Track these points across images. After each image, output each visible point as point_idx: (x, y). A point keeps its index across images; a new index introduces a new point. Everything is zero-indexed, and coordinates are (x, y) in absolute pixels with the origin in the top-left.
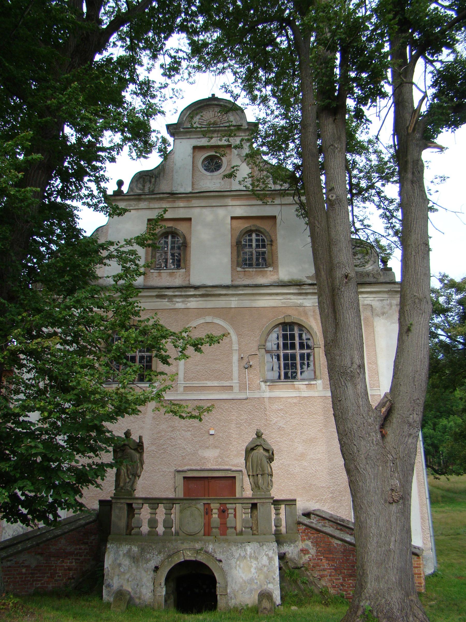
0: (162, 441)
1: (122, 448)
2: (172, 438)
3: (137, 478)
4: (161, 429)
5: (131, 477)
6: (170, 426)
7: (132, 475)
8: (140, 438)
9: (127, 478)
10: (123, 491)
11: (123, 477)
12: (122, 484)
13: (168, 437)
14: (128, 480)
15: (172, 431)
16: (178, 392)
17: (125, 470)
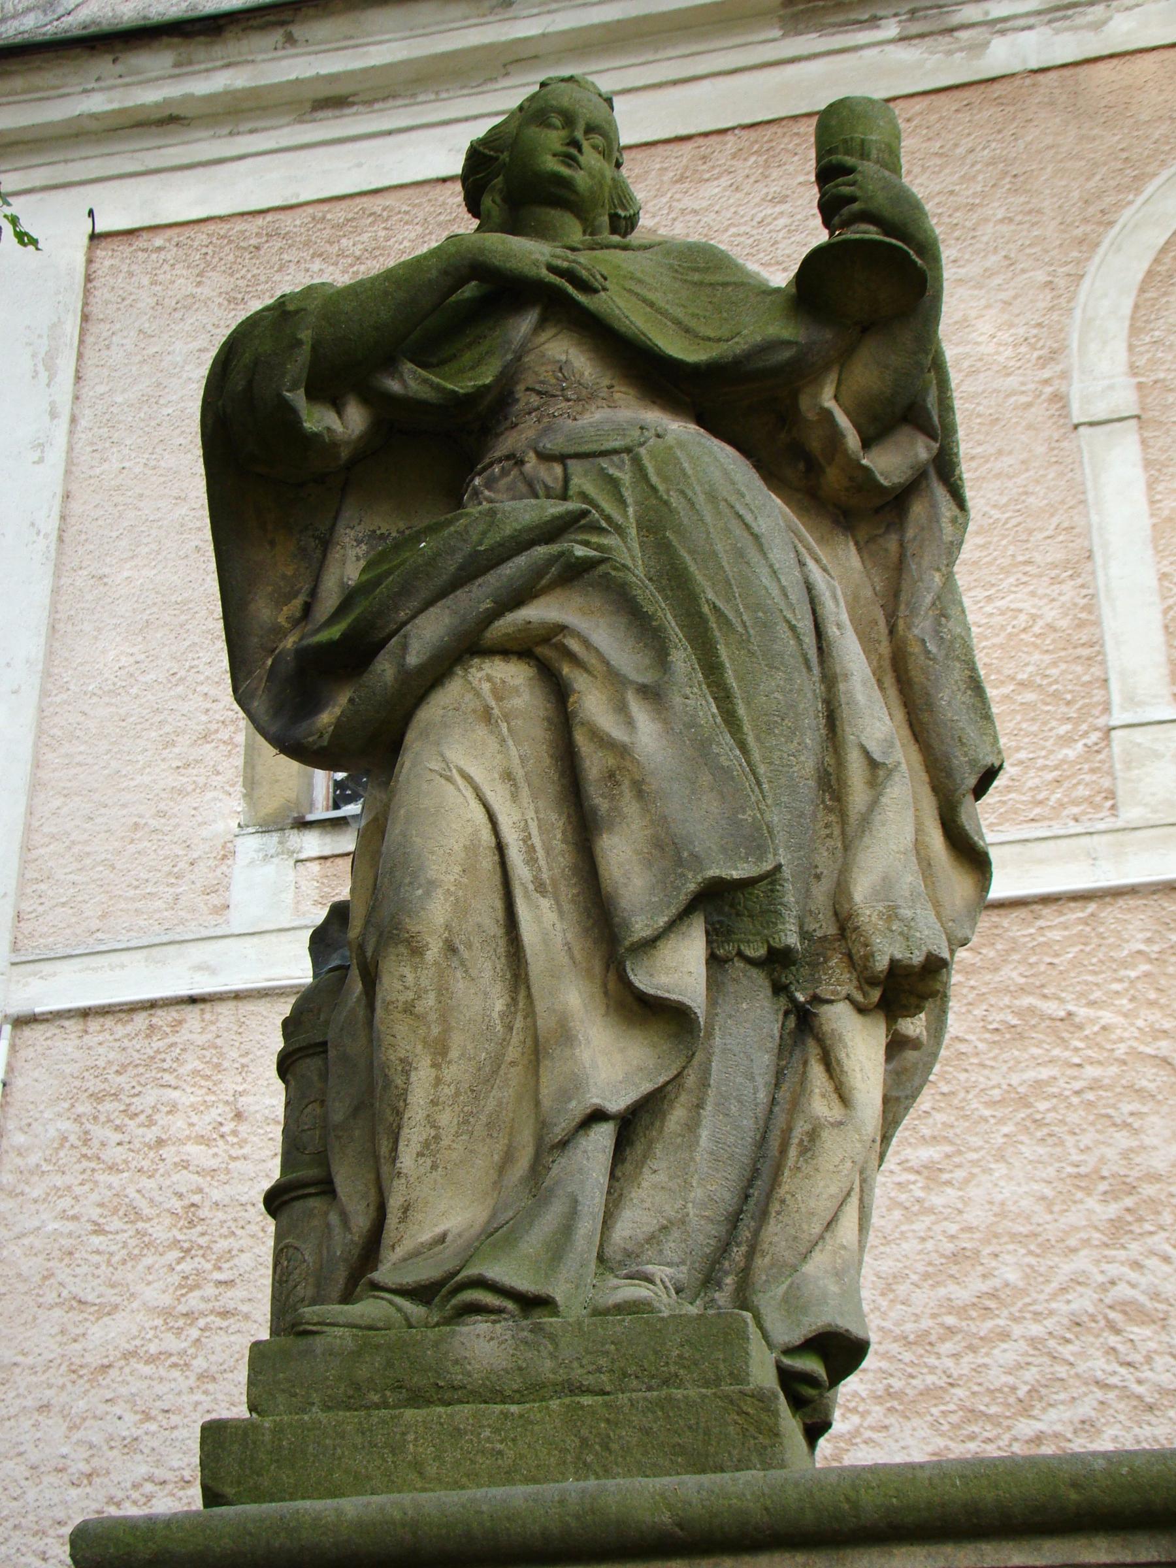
0: (1005, 1353)
1: (409, 381)
2: (1133, 1311)
3: (862, 1046)
4: (976, 1216)
5: (680, 968)
6: (1084, 1181)
7: (718, 904)
8: (845, 156)
9: (573, 997)
10: (484, 1345)
11: (481, 993)
12: (440, 1209)
13: (1083, 1302)
14: (610, 1065)
15: (1118, 1229)
16: (1130, 814)
17: (530, 825)
